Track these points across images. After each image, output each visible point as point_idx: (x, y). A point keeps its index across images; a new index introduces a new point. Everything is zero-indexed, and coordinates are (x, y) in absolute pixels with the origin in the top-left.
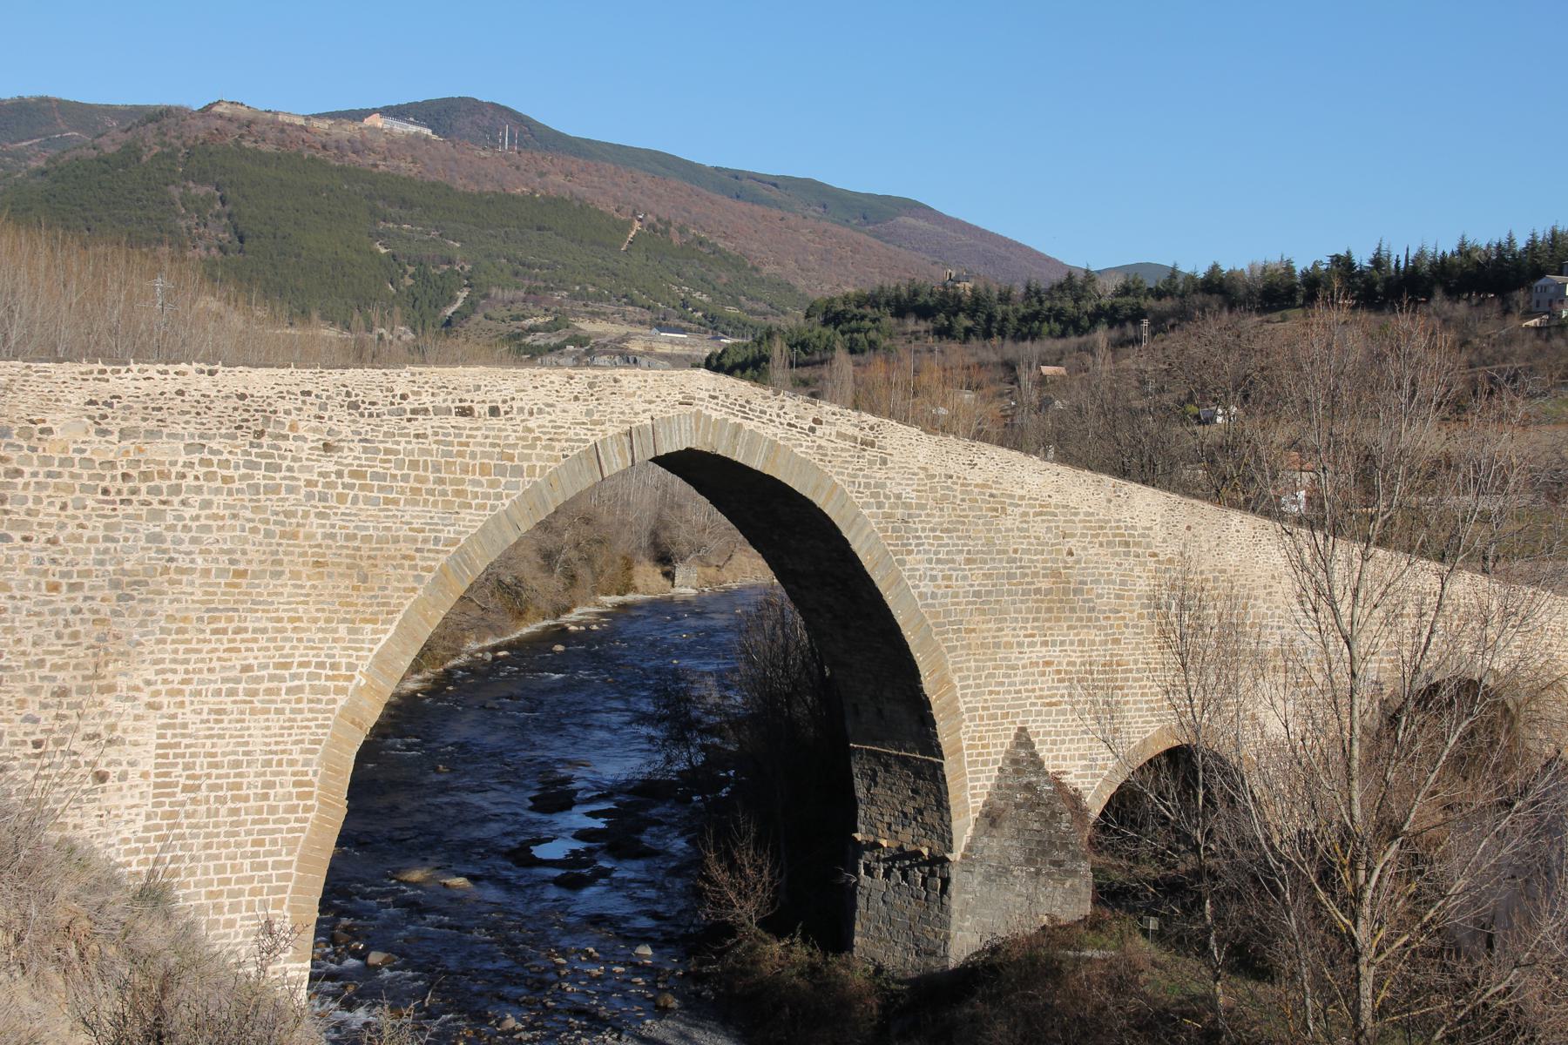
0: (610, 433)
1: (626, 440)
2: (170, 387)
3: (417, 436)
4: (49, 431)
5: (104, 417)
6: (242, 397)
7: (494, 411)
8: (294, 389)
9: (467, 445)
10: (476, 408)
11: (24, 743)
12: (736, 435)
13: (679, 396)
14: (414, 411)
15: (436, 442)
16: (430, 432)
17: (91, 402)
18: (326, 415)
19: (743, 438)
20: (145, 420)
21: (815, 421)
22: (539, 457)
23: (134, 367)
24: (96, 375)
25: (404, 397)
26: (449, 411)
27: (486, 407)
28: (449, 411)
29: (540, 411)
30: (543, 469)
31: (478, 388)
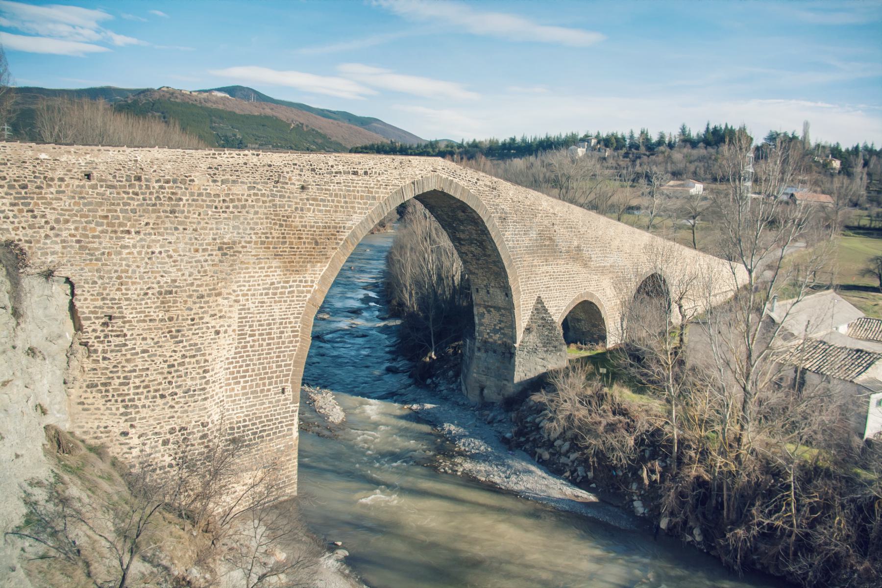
0: (407, 183)
1: (412, 185)
2: (241, 161)
3: (337, 183)
4: (193, 181)
5: (215, 174)
6: (270, 166)
7: (366, 173)
8: (290, 162)
9: (356, 187)
10: (359, 171)
11: (187, 319)
12: (451, 184)
13: (432, 169)
14: (336, 173)
15: (345, 186)
16: (342, 181)
17: (210, 168)
18: (303, 174)
19: (453, 185)
20: (231, 175)
21: (478, 179)
22: (382, 192)
23: (227, 152)
24: (211, 156)
25: (332, 166)
26: (349, 173)
27: (363, 171)
28: (349, 173)
29: (383, 173)
30: (383, 197)
31: (360, 163)
